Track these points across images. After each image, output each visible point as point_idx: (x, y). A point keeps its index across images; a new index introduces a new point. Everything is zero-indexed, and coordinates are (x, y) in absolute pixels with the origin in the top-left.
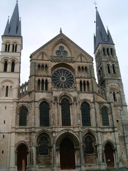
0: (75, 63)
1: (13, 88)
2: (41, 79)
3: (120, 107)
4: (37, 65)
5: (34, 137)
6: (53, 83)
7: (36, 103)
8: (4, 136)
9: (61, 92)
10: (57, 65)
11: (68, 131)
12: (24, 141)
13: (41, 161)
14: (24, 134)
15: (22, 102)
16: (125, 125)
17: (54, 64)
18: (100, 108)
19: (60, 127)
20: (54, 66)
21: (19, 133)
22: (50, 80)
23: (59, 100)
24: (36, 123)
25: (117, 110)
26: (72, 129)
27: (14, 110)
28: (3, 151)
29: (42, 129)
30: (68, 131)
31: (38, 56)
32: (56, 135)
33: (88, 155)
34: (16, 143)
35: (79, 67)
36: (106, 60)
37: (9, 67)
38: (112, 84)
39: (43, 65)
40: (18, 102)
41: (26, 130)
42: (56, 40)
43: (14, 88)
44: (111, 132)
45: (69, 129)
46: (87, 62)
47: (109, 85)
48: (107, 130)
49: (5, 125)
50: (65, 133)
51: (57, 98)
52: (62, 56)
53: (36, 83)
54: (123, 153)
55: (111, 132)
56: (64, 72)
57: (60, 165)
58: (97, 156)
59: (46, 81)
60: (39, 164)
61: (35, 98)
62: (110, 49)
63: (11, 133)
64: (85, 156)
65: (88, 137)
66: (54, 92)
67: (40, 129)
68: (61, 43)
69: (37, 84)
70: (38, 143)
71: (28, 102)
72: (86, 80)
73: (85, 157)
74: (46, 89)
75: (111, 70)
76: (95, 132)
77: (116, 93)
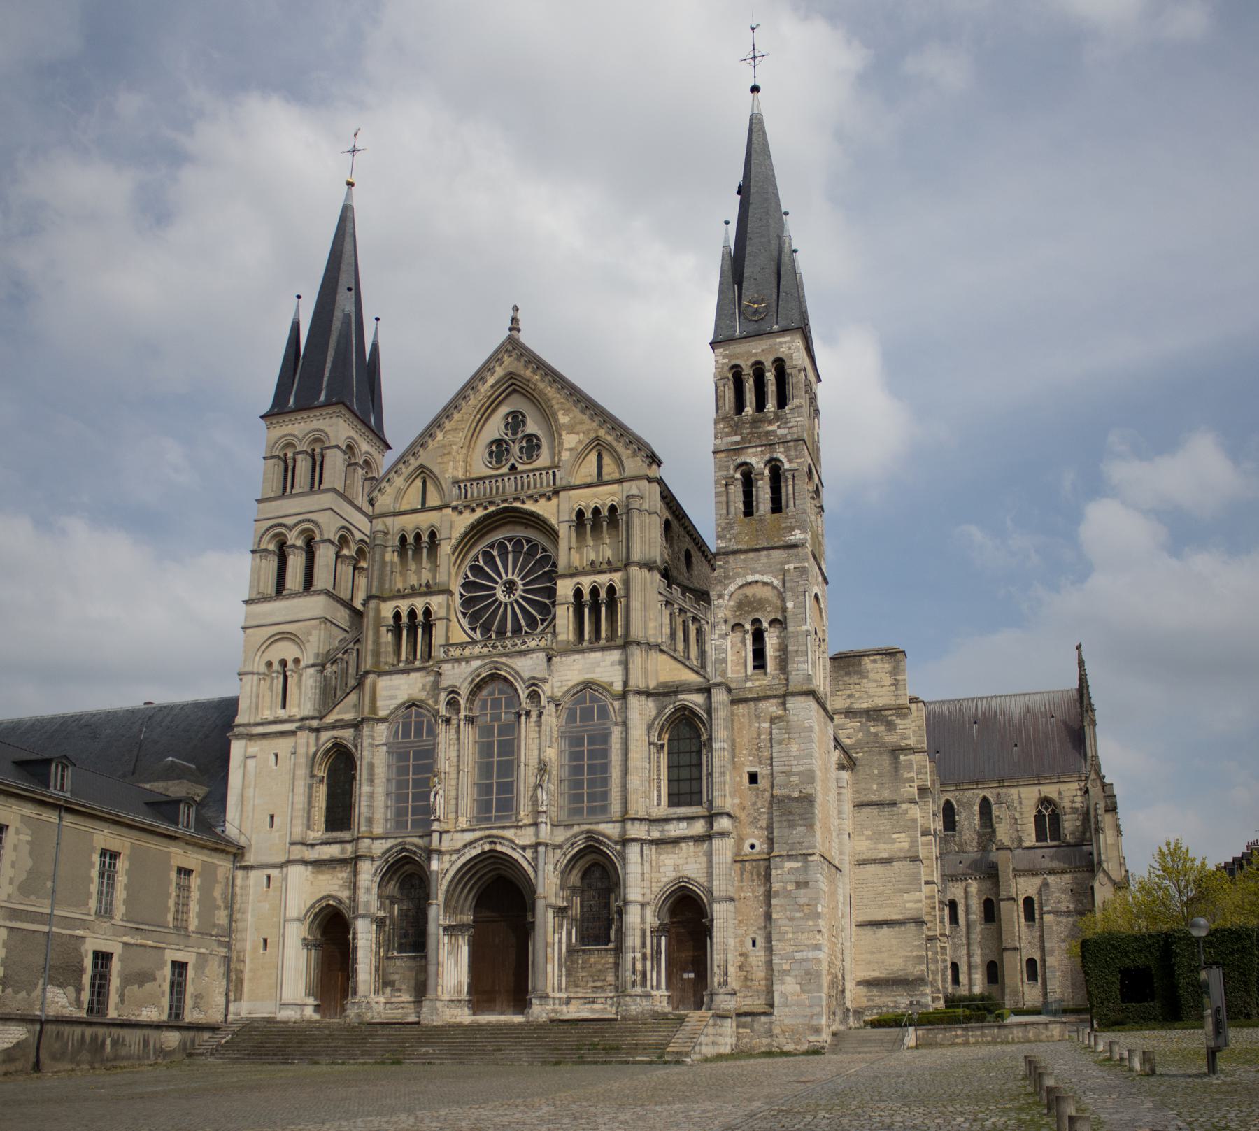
0: (561, 494)
1: (302, 664)
3: (775, 701)
6: (464, 614)
8: (269, 877)
9: (476, 664)
10: (480, 522)
11: (495, 843)
12: (334, 898)
13: (396, 977)
14: (335, 868)
16: (780, 801)
20: (466, 534)
21: (317, 864)
22: (440, 605)
25: (758, 717)
26: (509, 833)
28: (265, 941)
30: (495, 843)
31: (401, 493)
32: (446, 866)
33: (584, 951)
34: (308, 906)
35: (580, 514)
36: (737, 438)
37: (296, 563)
38: (750, 578)
39: (418, 537)
40: (317, 730)
41: (343, 851)
42: (484, 389)
43: (307, 667)
44: (697, 839)
45: (497, 837)
46: (620, 481)
47: (732, 588)
48: (675, 830)
49: (275, 834)
50: (483, 853)
51: (458, 694)
52: (513, 467)
53: (383, 630)
54: (757, 943)
55: (697, 839)
56: (517, 553)
57: (469, 993)
58: (619, 950)
59: (427, 612)
60: (388, 990)
61: (379, 703)
63: (289, 863)
64: (571, 951)
65: (595, 864)
66: (446, 668)
67: (390, 843)
68: (515, 397)
69: (388, 638)
71: (357, 725)
72: (603, 579)
73: (573, 962)
74: (429, 656)
76: (616, 843)
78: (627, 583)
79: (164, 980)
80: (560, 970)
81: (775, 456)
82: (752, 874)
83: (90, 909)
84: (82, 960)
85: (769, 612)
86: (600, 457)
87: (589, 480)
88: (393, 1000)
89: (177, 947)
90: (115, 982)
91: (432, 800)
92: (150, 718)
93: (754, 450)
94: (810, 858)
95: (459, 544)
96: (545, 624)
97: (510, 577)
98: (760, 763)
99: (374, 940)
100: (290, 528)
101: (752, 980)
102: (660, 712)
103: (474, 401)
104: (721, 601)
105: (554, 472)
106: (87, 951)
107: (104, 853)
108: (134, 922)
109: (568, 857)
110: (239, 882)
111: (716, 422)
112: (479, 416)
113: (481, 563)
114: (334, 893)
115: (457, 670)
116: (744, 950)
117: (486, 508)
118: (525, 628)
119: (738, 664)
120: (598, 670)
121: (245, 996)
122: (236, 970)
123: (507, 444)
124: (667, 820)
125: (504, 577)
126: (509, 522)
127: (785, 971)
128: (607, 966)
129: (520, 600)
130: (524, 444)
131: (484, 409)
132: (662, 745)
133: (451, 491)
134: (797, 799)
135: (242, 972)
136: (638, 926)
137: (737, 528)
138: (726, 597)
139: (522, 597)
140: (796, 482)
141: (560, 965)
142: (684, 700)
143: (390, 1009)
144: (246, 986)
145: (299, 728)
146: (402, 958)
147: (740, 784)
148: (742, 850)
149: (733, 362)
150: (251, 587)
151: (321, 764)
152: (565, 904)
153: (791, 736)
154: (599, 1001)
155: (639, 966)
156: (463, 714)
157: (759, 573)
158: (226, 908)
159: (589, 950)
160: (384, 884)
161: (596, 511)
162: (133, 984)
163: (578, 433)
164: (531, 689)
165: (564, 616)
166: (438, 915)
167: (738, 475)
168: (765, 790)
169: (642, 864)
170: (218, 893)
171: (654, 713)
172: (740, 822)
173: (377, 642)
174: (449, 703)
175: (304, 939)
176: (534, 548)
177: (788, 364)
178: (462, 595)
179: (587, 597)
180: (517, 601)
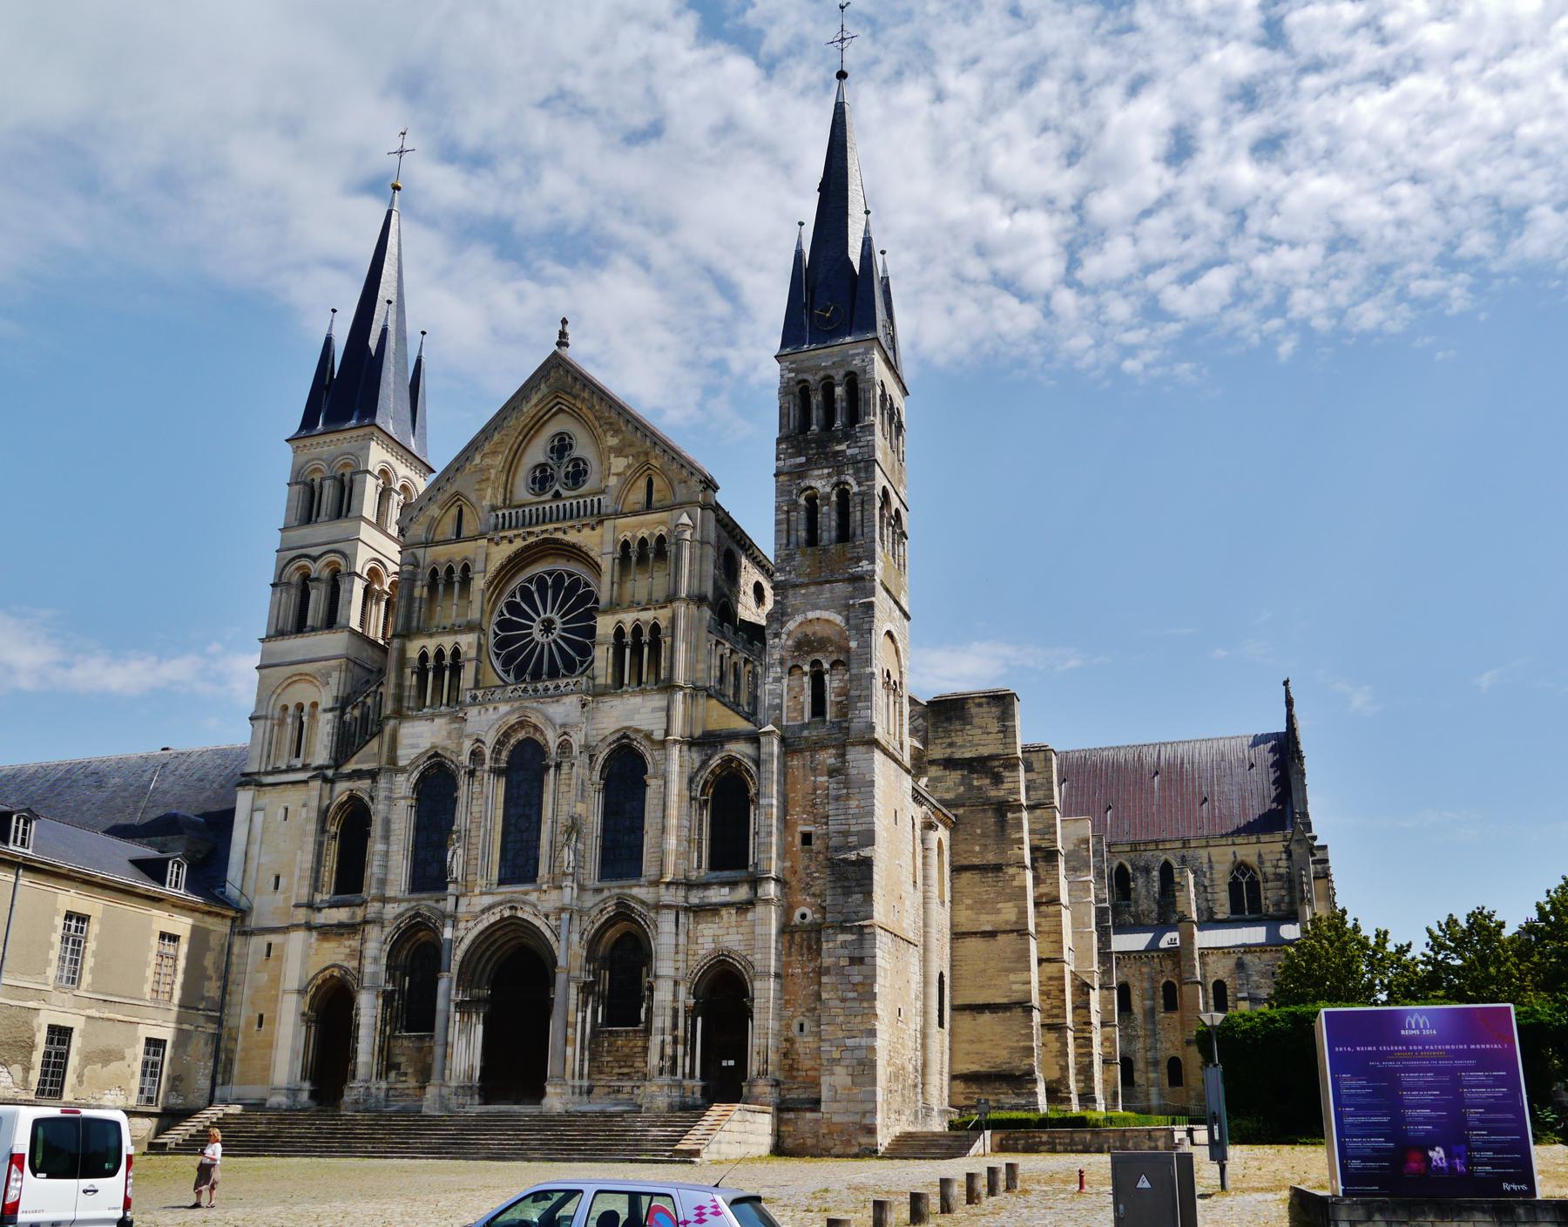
0: (605, 522)
1: (320, 708)
2: (431, 645)
3: (833, 751)
4: (424, 576)
5: (376, 944)
6: (497, 655)
7: (401, 778)
8: (270, 945)
9: (504, 708)
10: (517, 554)
11: (516, 909)
12: (340, 967)
13: (402, 1059)
14: (342, 934)
15: (357, 775)
17: (502, 553)
18: (706, 774)
19: (482, 894)
20: (503, 567)
23: (497, 752)
24: (391, 877)
25: (814, 770)
26: (533, 897)
27: (308, 819)
28: (261, 1017)
29: (414, 904)
32: (461, 933)
33: (611, 1033)
36: (803, 459)
38: (811, 615)
39: (450, 570)
40: (331, 782)
41: (354, 914)
43: (325, 711)
45: (518, 902)
47: (791, 625)
49: (280, 896)
50: (502, 919)
51: (483, 743)
52: (557, 496)
58: (648, 1031)
59: (456, 652)
60: (393, 1074)
61: (400, 752)
62: (839, 375)
67: (404, 906)
68: (561, 416)
69: (411, 680)
70: (398, 973)
71: (373, 775)
72: (648, 616)
74: (454, 700)
75: (828, 519)
76: (649, 910)
77: (826, 666)
78: (673, 621)
79: (135, 1060)
80: (582, 1054)
81: (843, 479)
82: (801, 948)
83: (47, 978)
84: (34, 1035)
85: (831, 652)
86: (650, 484)
87: (638, 507)
88: (399, 1086)
89: (154, 1022)
90: (73, 1061)
91: (449, 860)
92: (164, 766)
93: (820, 472)
94: (867, 931)
95: (495, 577)
96: (585, 665)
97: (548, 615)
98: (815, 822)
99: (379, 1016)
100: (315, 559)
101: (798, 1070)
102: (704, 764)
103: (517, 423)
104: (777, 640)
105: (599, 500)
106: (40, 1025)
107: (69, 916)
108: (102, 993)
109: (596, 926)
110: (236, 950)
111: (779, 441)
112: (521, 438)
113: (518, 599)
114: (340, 963)
115: (483, 717)
116: (790, 1035)
117: (524, 539)
118: (562, 671)
119: (795, 710)
120: (636, 716)
121: (235, 1080)
122: (226, 1049)
123: (552, 469)
124: (706, 885)
125: (543, 616)
126: (551, 554)
127: (834, 1060)
128: (636, 1050)
129: (559, 640)
130: (570, 469)
131: (526, 430)
132: (706, 801)
133: (488, 520)
134: (853, 863)
135: (233, 1051)
136: (669, 1005)
137: (798, 558)
138: (784, 636)
139: (562, 638)
140: (866, 507)
141: (582, 1048)
142: (731, 751)
143: (393, 1096)
144: (237, 1068)
145: (312, 777)
146: (410, 1037)
147: (792, 844)
148: (792, 919)
149: (800, 377)
150: (269, 624)
151: (334, 819)
152: (591, 979)
153: (850, 791)
154: (625, 1090)
155: (669, 1051)
156: (486, 767)
157: (820, 609)
158: (219, 979)
159: (616, 1031)
160: (395, 952)
161: (643, 541)
162: (94, 1063)
163: (627, 457)
164: (562, 738)
165: (602, 657)
166: (450, 989)
167: (802, 501)
168: (819, 852)
169: (677, 934)
170: (209, 961)
171: (697, 765)
172: (789, 888)
173: (400, 686)
174: (473, 753)
175: (304, 1014)
176: (576, 583)
177: (861, 377)
178: (495, 633)
179: (628, 639)
180: (555, 641)
